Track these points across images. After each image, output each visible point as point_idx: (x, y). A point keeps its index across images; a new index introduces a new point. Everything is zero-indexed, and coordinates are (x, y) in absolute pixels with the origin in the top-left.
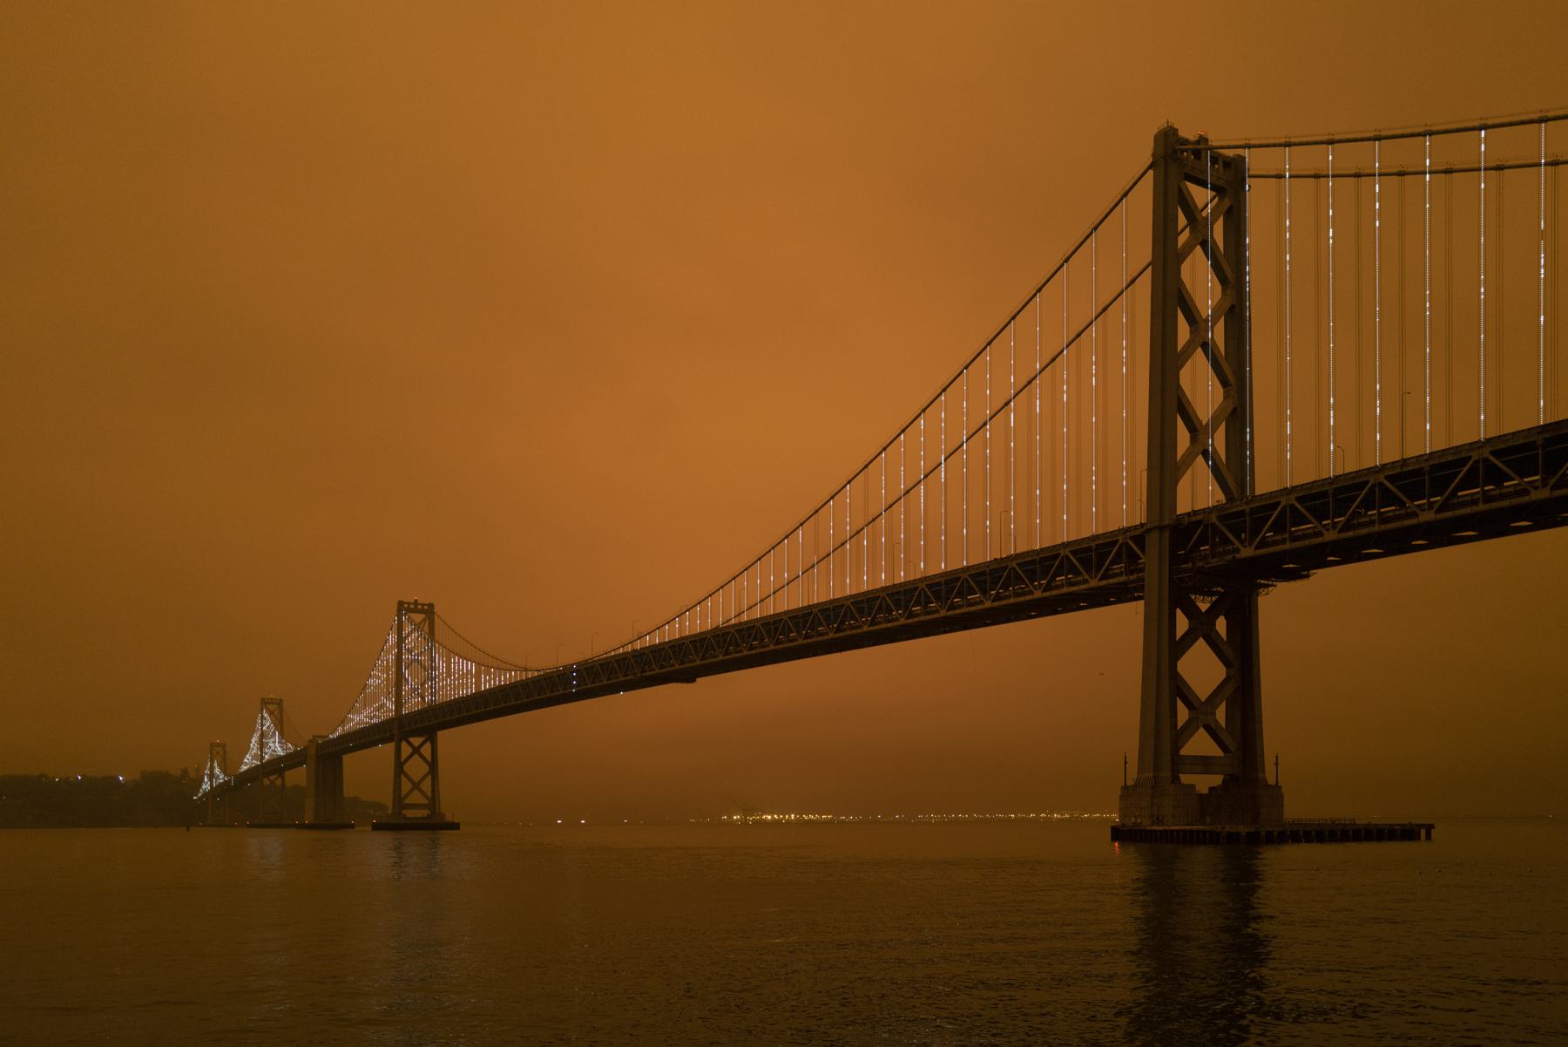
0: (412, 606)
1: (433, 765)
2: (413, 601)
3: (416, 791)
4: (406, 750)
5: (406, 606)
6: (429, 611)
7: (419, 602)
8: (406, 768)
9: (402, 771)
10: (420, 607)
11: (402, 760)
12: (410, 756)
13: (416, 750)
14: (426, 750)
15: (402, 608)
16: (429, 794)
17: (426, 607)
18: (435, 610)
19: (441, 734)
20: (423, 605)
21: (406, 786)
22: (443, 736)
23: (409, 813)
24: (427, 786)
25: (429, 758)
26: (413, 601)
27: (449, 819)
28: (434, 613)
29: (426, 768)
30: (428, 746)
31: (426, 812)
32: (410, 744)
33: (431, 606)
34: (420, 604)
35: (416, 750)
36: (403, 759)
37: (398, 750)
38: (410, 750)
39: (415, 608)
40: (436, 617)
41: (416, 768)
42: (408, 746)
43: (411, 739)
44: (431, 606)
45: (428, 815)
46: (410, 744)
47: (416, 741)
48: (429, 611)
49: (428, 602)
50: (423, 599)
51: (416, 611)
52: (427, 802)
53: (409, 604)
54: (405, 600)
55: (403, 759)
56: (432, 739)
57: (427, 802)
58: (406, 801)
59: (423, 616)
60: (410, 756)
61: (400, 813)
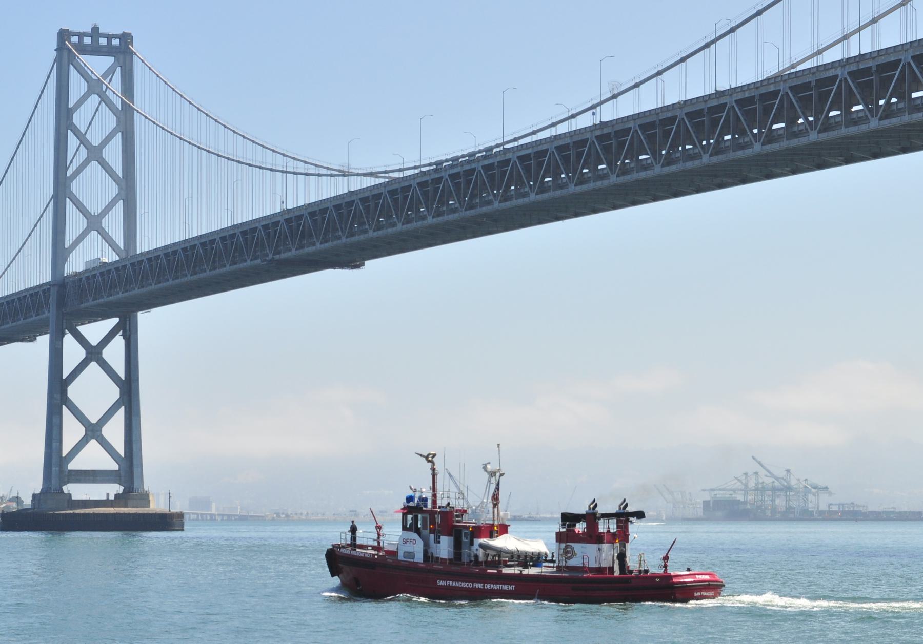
0: (87, 40)
2: (89, 31)
3: (93, 443)
4: (73, 352)
7: (101, 31)
8: (73, 392)
9: (65, 401)
10: (103, 41)
11: (66, 373)
13: (94, 354)
16: (120, 447)
17: (116, 42)
20: (109, 37)
21: (72, 432)
22: (147, 320)
23: (78, 491)
24: (115, 432)
25: (120, 369)
26: (88, 30)
27: (157, 505)
28: (132, 53)
29: (114, 393)
30: (119, 342)
31: (113, 489)
33: (126, 38)
34: (103, 36)
35: (94, 354)
36: (66, 373)
40: (136, 62)
43: (81, 328)
44: (126, 38)
45: (117, 496)
47: (94, 331)
49: (120, 32)
52: (115, 466)
53: (81, 35)
54: (72, 29)
55: (66, 373)
56: (128, 330)
57: (115, 466)
58: (73, 465)
59: (109, 61)
61: (62, 492)
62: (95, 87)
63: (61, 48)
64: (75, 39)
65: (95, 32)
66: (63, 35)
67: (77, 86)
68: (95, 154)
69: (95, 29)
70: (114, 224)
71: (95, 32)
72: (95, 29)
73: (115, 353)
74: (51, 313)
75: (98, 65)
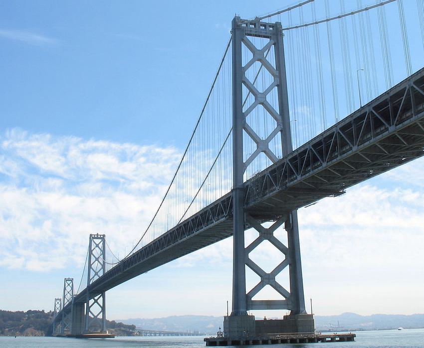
0: (96, 236)
1: (103, 308)
5: (93, 236)
6: (103, 238)
10: (99, 236)
13: (96, 301)
14: (100, 301)
15: (92, 237)
17: (102, 236)
18: (106, 238)
20: (100, 235)
22: (107, 293)
30: (101, 298)
33: (104, 236)
44: (104, 236)
48: (103, 238)
51: (97, 238)
59: (101, 240)
62: (97, 246)
63: (90, 238)
66: (91, 235)
67: (93, 246)
68: (97, 259)
73: (100, 301)
75: (97, 241)
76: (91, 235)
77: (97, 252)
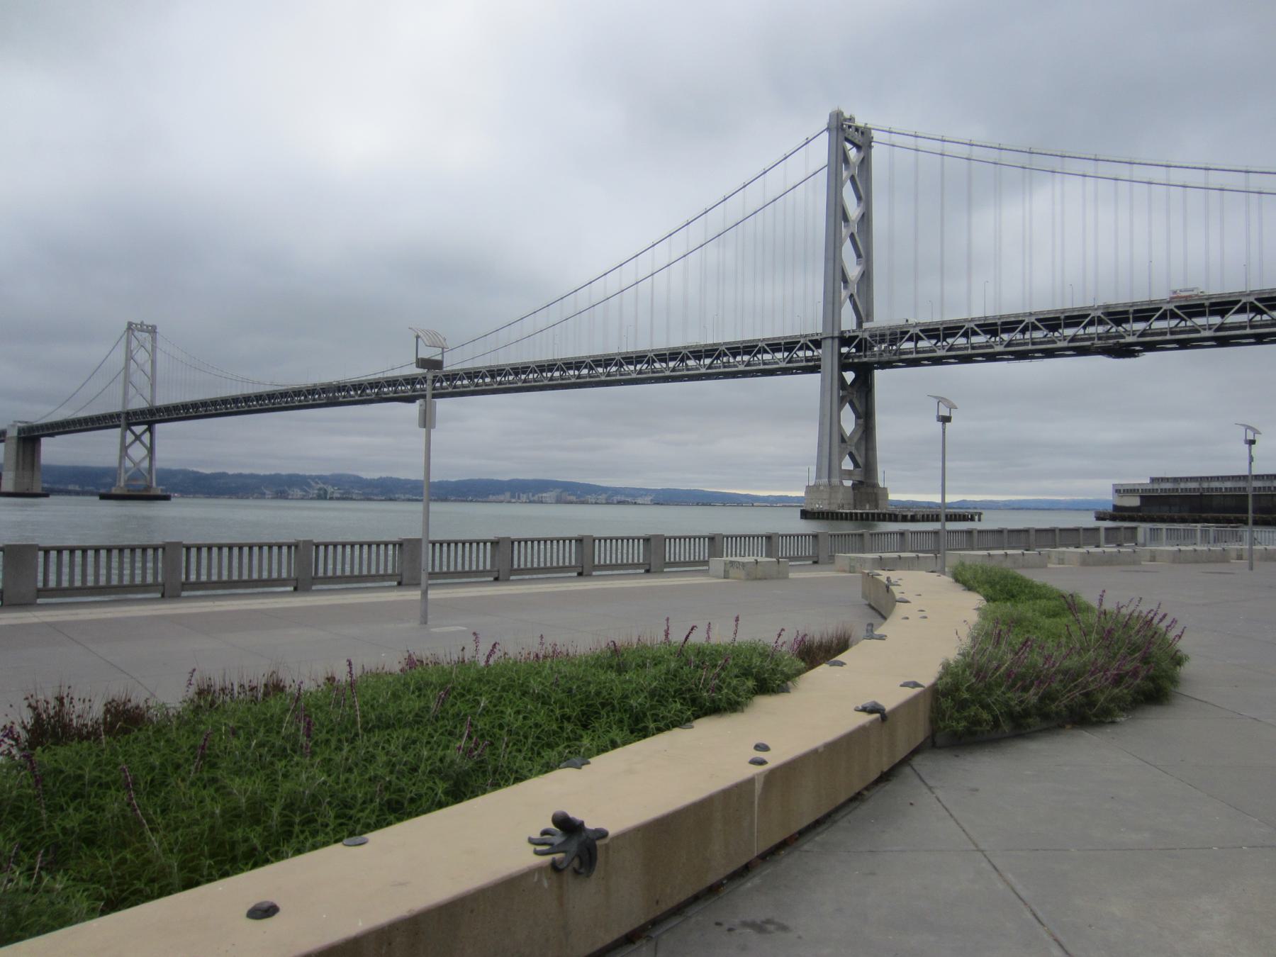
2: (139, 323)
6: (153, 330)
9: (127, 454)
12: (133, 442)
13: (138, 438)
19: (158, 427)
22: (159, 427)
26: (139, 323)
28: (156, 332)
30: (147, 435)
32: (133, 432)
37: (123, 438)
38: (133, 437)
39: (143, 328)
41: (138, 452)
42: (132, 435)
46: (133, 432)
47: (138, 429)
48: (153, 330)
50: (148, 322)
53: (136, 325)
54: (134, 322)
56: (150, 430)
60: (133, 442)
64: (134, 326)
65: (142, 324)
66: (130, 324)
67: (134, 343)
69: (142, 323)
70: (147, 393)
71: (142, 324)
72: (142, 323)
73: (146, 438)
74: (123, 421)
76: (130, 324)
77: (142, 356)
